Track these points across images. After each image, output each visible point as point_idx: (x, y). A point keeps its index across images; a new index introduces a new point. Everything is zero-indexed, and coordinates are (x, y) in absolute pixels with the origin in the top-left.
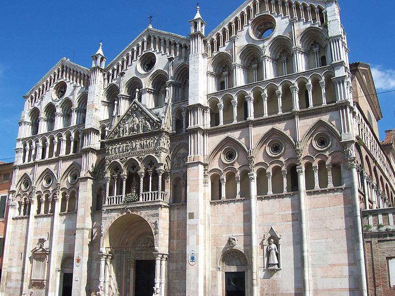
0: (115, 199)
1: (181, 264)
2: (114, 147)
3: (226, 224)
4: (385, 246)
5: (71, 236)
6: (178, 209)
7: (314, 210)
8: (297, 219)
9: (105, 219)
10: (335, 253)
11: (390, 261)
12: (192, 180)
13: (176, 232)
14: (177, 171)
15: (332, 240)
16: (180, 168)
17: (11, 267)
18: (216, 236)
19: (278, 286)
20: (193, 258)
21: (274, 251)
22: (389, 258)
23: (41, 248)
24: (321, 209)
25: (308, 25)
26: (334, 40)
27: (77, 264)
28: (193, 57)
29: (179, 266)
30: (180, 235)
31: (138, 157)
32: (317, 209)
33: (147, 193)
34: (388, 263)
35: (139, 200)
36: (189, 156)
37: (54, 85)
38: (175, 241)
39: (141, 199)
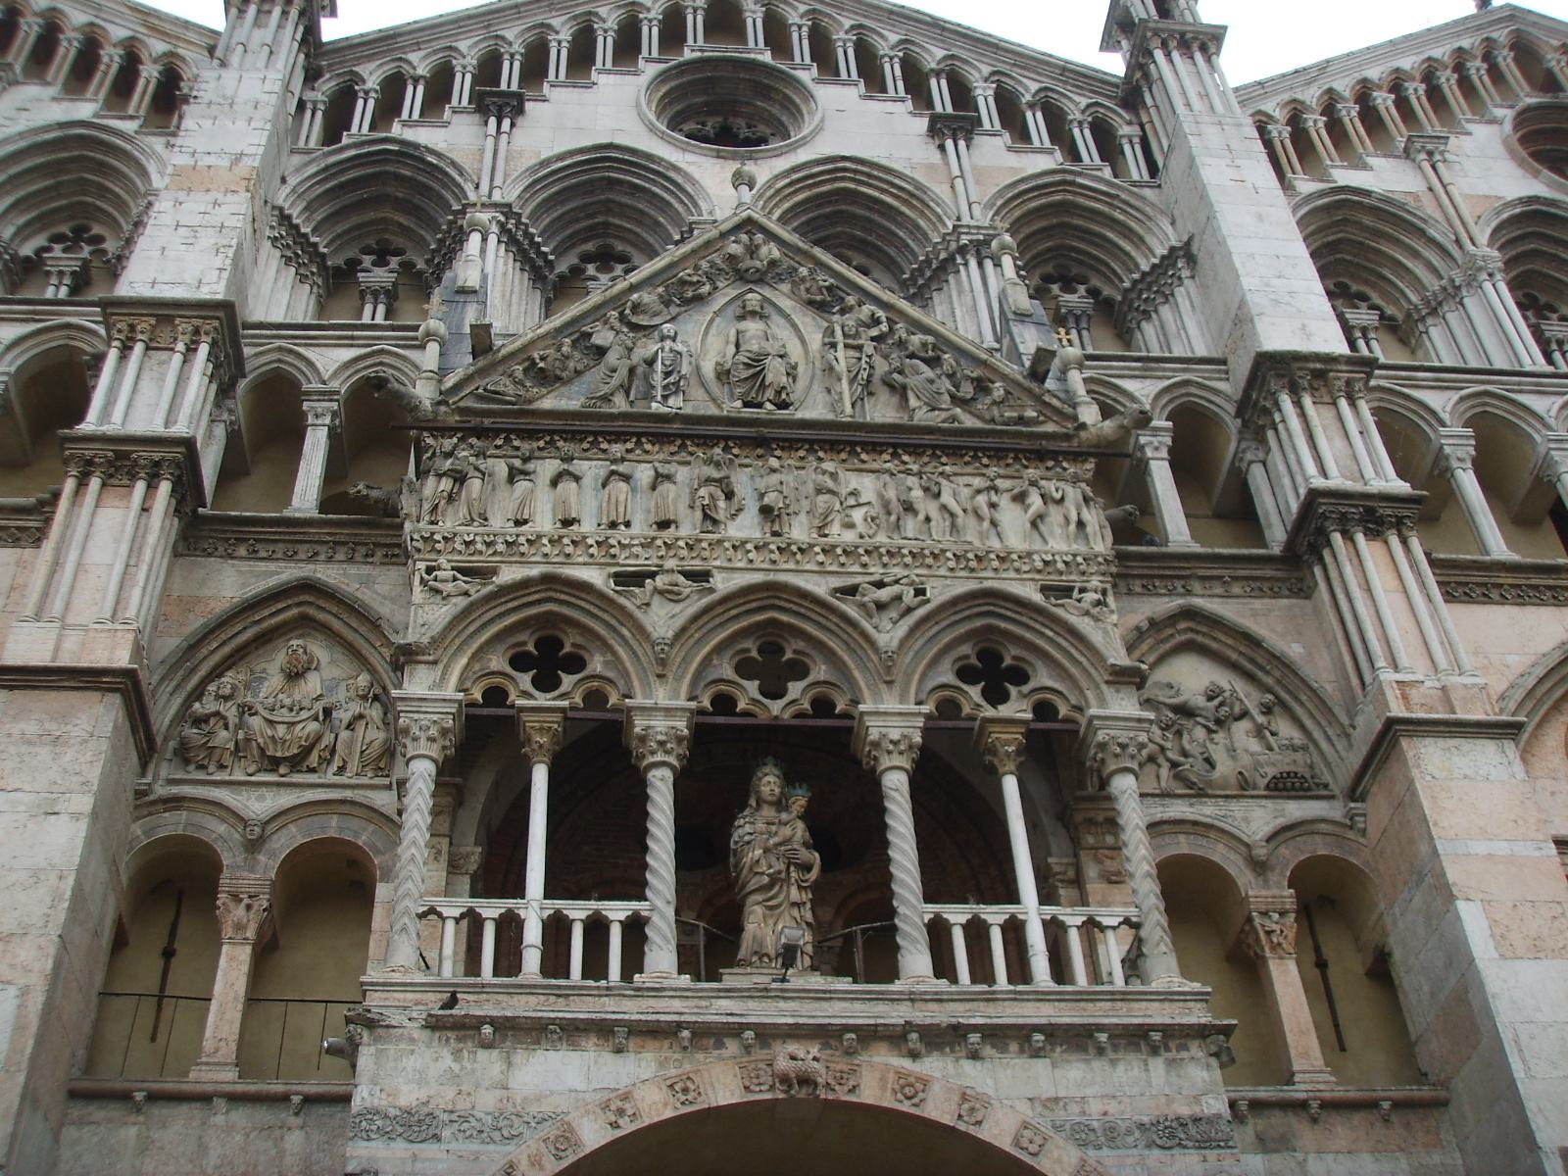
0: (533, 933)
2: (548, 467)
9: (418, 1125)
12: (1490, 857)
16: (1199, 792)
28: (1211, 132)
31: (851, 591)
33: (994, 915)
35: (891, 973)
36: (1388, 676)
39: (916, 961)
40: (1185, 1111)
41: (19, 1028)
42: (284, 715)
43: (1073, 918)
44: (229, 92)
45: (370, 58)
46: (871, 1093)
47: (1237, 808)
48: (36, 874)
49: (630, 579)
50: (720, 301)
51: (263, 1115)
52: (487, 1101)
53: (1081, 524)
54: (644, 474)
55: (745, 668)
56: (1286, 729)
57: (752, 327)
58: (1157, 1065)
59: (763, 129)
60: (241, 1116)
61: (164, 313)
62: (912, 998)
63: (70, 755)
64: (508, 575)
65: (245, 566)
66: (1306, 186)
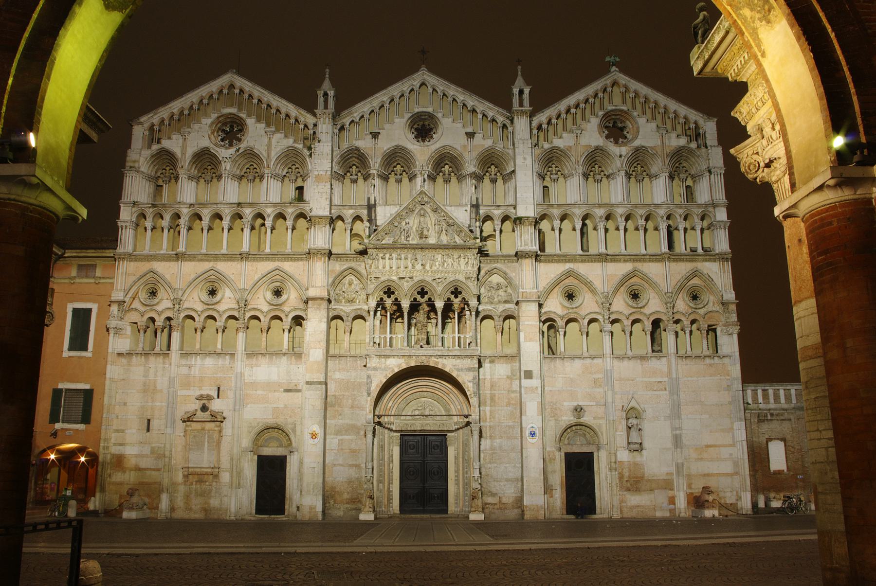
0: (388, 340)
1: (497, 441)
3: (570, 388)
4: (765, 427)
5: (276, 394)
6: (492, 362)
7: (685, 379)
8: (665, 389)
9: (375, 369)
10: (711, 432)
11: (769, 443)
13: (488, 396)
14: (488, 307)
15: (707, 416)
17: (121, 445)
18: (553, 404)
19: (641, 471)
20: (533, 434)
21: (635, 426)
22: (771, 440)
23: (204, 408)
24: (695, 379)
25: (683, 141)
26: (715, 173)
27: (311, 441)
28: (521, 146)
29: (495, 444)
30: (497, 400)
32: (690, 379)
34: (767, 445)
37: (214, 116)
38: (488, 409)
40: (472, 367)
41: (323, 354)
42: (349, 293)
43: (462, 336)
44: (322, 150)
45: (346, 117)
46: (431, 365)
47: (497, 306)
48: (321, 332)
49: (400, 278)
50: (417, 211)
51: (354, 358)
52: (383, 366)
53: (473, 264)
54: (403, 256)
55: (419, 293)
56: (509, 290)
57: (422, 219)
58: (470, 360)
59: (432, 126)
60: (351, 359)
61: (321, 217)
62: (438, 350)
63: (322, 312)
64: (382, 279)
65: (340, 263)
66: (546, 146)
